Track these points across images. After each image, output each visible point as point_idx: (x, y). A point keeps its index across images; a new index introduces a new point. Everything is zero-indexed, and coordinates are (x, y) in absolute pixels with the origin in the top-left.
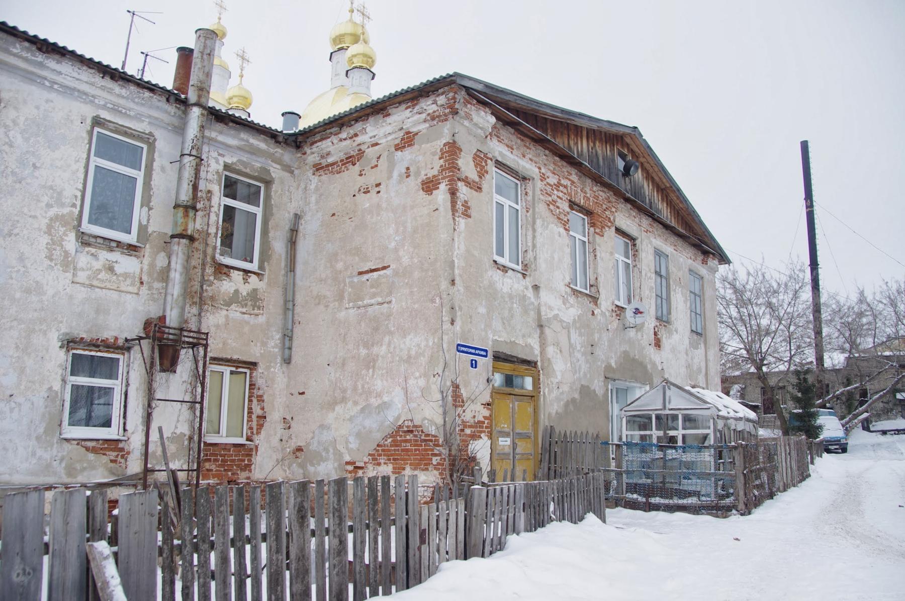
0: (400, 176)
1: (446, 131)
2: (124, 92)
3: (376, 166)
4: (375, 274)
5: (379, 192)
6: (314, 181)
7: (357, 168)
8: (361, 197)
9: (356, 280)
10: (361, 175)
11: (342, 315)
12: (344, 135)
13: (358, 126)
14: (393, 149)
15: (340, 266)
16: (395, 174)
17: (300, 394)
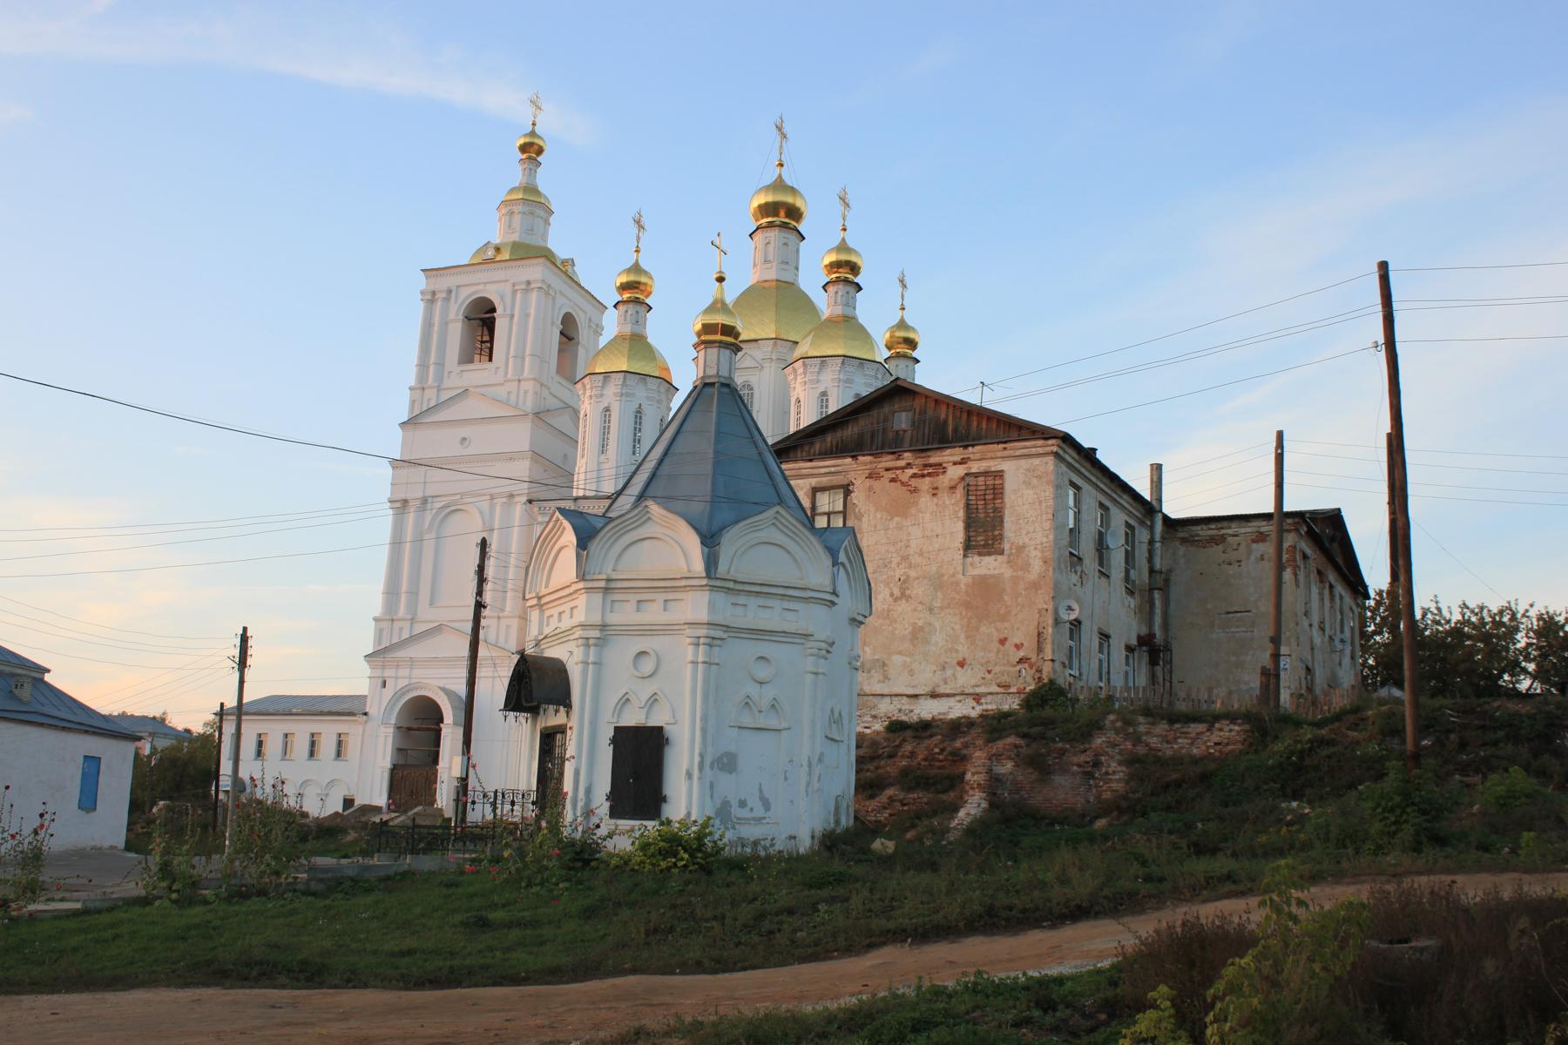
0: (1256, 559)
2: (1134, 505)
3: (1237, 549)
4: (1239, 615)
5: (1240, 566)
6: (1182, 550)
7: (1220, 547)
8: (1225, 567)
9: (1223, 616)
10: (1224, 552)
11: (1214, 636)
12: (1213, 527)
13: (1225, 524)
14: (1249, 542)
15: (1209, 606)
16: (1253, 557)
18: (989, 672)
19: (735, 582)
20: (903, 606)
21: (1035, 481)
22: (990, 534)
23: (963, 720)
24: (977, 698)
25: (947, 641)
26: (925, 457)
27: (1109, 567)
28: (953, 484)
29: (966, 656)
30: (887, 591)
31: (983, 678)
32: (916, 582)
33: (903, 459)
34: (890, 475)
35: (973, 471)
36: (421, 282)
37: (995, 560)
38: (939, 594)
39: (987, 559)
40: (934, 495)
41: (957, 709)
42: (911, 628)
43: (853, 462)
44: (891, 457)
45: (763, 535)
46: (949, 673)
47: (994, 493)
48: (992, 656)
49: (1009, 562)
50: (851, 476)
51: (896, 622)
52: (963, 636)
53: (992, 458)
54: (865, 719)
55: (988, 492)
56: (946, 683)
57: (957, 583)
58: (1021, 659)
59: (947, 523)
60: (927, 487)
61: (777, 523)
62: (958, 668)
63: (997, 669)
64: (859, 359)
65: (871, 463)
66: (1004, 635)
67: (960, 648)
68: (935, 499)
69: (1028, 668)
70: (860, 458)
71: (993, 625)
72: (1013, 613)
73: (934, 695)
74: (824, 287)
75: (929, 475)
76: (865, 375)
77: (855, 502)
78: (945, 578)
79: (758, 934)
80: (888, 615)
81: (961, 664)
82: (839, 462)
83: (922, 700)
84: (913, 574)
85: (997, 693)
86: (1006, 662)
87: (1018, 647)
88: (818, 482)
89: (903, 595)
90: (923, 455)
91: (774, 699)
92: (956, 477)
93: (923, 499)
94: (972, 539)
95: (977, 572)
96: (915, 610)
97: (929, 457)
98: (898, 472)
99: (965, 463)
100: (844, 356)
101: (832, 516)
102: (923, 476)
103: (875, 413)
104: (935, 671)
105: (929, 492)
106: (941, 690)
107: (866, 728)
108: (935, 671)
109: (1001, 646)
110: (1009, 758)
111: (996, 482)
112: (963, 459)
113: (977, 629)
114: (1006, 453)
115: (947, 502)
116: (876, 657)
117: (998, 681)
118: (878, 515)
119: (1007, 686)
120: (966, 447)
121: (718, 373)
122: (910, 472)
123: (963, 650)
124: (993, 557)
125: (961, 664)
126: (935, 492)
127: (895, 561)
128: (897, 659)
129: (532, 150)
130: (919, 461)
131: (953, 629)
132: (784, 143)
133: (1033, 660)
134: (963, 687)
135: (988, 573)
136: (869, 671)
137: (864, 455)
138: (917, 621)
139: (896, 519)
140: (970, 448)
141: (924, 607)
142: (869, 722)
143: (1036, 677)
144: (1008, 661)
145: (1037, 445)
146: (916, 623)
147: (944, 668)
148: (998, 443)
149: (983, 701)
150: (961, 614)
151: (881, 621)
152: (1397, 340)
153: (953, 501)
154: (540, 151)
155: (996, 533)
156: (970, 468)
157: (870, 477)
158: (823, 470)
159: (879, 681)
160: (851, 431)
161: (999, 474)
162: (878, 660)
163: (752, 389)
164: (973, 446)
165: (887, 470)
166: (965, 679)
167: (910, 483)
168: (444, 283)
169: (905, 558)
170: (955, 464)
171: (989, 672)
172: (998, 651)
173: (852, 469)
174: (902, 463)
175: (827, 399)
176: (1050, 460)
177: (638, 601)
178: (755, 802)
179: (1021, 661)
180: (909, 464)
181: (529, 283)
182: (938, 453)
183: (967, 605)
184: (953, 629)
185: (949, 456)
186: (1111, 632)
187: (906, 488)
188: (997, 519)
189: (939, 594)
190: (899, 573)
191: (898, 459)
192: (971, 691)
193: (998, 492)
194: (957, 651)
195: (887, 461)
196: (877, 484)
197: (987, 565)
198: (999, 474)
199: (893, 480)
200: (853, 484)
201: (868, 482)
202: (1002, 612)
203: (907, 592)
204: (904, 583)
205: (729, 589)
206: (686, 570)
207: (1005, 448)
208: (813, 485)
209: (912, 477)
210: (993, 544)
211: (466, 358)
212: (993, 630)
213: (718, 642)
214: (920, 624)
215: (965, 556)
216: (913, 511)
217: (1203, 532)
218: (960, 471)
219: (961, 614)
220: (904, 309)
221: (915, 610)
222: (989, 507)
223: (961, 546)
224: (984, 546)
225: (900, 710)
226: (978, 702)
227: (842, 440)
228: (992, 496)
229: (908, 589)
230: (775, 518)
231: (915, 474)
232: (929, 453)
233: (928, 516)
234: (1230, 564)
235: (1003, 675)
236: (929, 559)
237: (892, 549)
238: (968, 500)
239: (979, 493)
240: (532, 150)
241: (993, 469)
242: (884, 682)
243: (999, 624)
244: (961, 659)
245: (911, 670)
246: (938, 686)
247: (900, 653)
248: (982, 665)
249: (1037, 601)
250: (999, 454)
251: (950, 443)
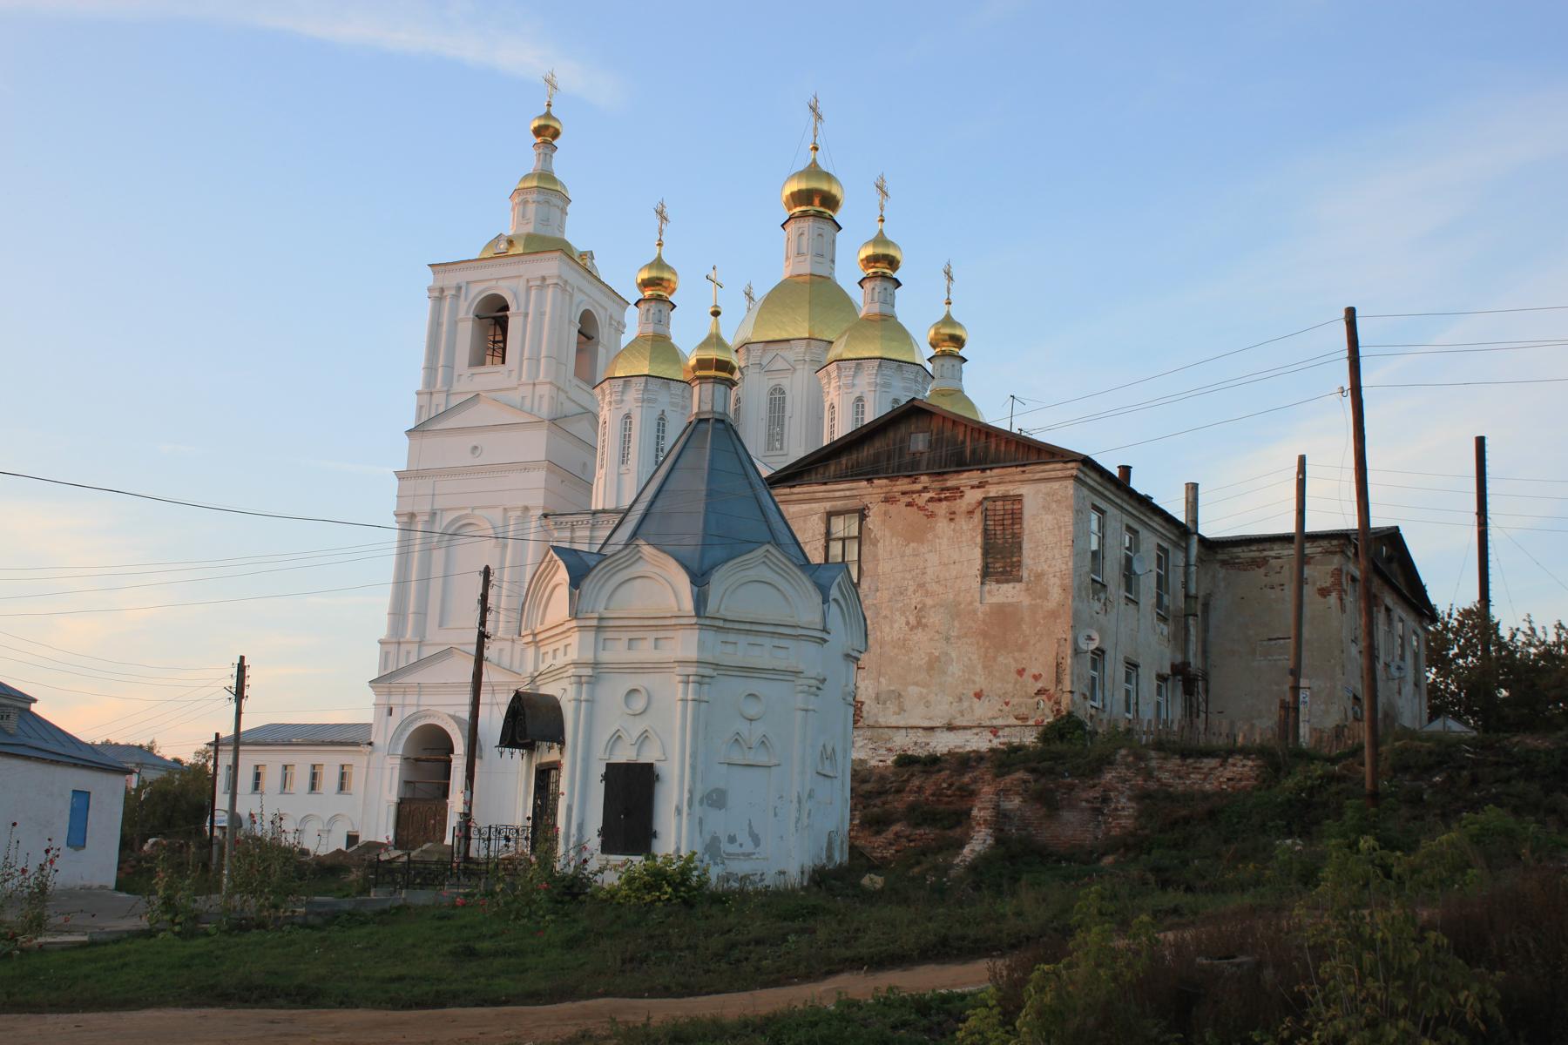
1: (1335, 561)
2: (1167, 527)
4: (1282, 641)
5: (1282, 590)
6: (1222, 573)
7: (1262, 570)
9: (1265, 643)
10: (1266, 576)
12: (1254, 548)
13: (1267, 545)
17: (1219, 712)
18: (1007, 704)
19: (725, 620)
20: (919, 635)
21: (1054, 506)
22: (1008, 560)
23: (972, 755)
24: (994, 731)
25: (964, 672)
27: (1138, 593)
28: (970, 508)
29: (983, 687)
30: (903, 620)
31: (1001, 710)
32: (933, 609)
33: (919, 483)
34: (906, 499)
35: (991, 495)
36: (429, 278)
37: (1014, 588)
38: (956, 623)
39: (1005, 587)
40: (951, 520)
41: (979, 743)
42: (927, 658)
43: (869, 486)
44: (907, 480)
45: (752, 574)
46: (966, 704)
47: (1013, 518)
48: (1010, 687)
49: (1027, 590)
50: (866, 500)
51: (912, 651)
52: (980, 666)
53: (1010, 482)
54: (880, 752)
55: (1006, 517)
56: (963, 716)
57: (975, 612)
58: (1039, 691)
59: (965, 549)
60: (944, 512)
61: (768, 562)
62: (975, 700)
63: (1014, 701)
64: (896, 361)
65: (886, 486)
66: (1023, 666)
67: (977, 679)
68: (953, 525)
69: (1046, 700)
70: (875, 481)
71: (1011, 655)
72: (1032, 642)
73: (951, 728)
74: (860, 283)
75: (946, 499)
76: (903, 379)
77: (871, 527)
78: (962, 606)
79: (726, 962)
80: (904, 645)
81: (978, 695)
82: (854, 485)
83: (938, 733)
84: (929, 602)
85: (1015, 726)
86: (1024, 694)
87: (1036, 678)
88: (832, 506)
89: (919, 623)
90: (940, 478)
91: (764, 736)
92: (973, 502)
93: (939, 524)
94: (990, 565)
95: (994, 600)
96: (931, 639)
97: (946, 480)
98: (914, 496)
99: (983, 487)
100: (881, 358)
101: (847, 542)
102: (940, 500)
103: (891, 434)
104: (951, 703)
105: (945, 517)
106: (958, 722)
107: (881, 761)
108: (951, 703)
109: (1019, 678)
110: (1017, 793)
111: (1015, 507)
112: (980, 483)
113: (995, 659)
115: (965, 528)
116: (892, 688)
117: (1016, 714)
118: (894, 541)
119: (1025, 719)
120: (983, 470)
121: (712, 409)
122: (927, 496)
123: (981, 681)
124: (1011, 585)
125: (978, 695)
126: (953, 516)
127: (911, 589)
128: (913, 690)
129: (547, 133)
130: (937, 485)
131: (970, 659)
132: (819, 125)
133: (1052, 691)
134: (981, 719)
135: (1006, 600)
136: (884, 703)
137: (879, 478)
138: (934, 651)
139: (912, 545)
140: (988, 472)
141: (941, 636)
142: (884, 755)
143: (1054, 709)
144: (1026, 692)
145: (1055, 469)
146: (933, 653)
147: (960, 700)
148: (1017, 466)
149: (1000, 733)
150: (978, 643)
151: (896, 651)
152: (1362, 384)
153: (971, 526)
154: (556, 134)
155: (1015, 559)
156: (989, 492)
157: (886, 500)
158: (842, 494)
159: (895, 713)
160: (867, 452)
161: (1018, 499)
162: (893, 691)
163: (784, 393)
164: (991, 469)
165: (904, 493)
166: (982, 711)
167: (927, 507)
168: (452, 279)
169: (921, 586)
170: (973, 487)
171: (1007, 704)
172: (1016, 683)
173: (867, 492)
174: (918, 487)
175: (863, 405)
176: (1070, 484)
177: (630, 640)
178: (743, 837)
179: (1039, 693)
180: (925, 488)
181: (544, 279)
182: (955, 476)
183: (985, 635)
184: (970, 659)
185: (965, 479)
186: (1140, 661)
187: (923, 512)
188: (1016, 546)
189: (956, 623)
190: (915, 600)
191: (914, 482)
192: (988, 723)
193: (1016, 517)
194: (974, 682)
195: (903, 485)
196: (892, 508)
197: (1005, 593)
198: (1018, 499)
199: (909, 504)
200: (869, 509)
201: (884, 506)
202: (1020, 642)
203: (924, 621)
204: (920, 610)
205: (718, 627)
206: (676, 609)
207: (1024, 472)
208: (828, 509)
209: (929, 501)
210: (1012, 571)
211: (478, 361)
212: (1011, 661)
213: (707, 680)
214: (937, 654)
215: (982, 583)
216: (930, 536)
217: (1244, 554)
218: (978, 495)
219: (978, 643)
220: (950, 303)
221: (931, 639)
222: (1007, 532)
223: (978, 573)
224: (1002, 573)
225: (916, 743)
226: (995, 735)
227: (858, 462)
228: (1010, 521)
229: (924, 617)
230: (766, 556)
231: (931, 498)
232: (946, 477)
233: (945, 541)
234: (1272, 588)
235: (1021, 706)
236: (946, 586)
237: (908, 576)
238: (985, 525)
239: (997, 518)
240: (547, 133)
241: (1011, 493)
242: (899, 714)
243: (1016, 654)
244: (978, 690)
245: (927, 701)
246: (955, 719)
247: (916, 684)
248: (1000, 697)
249: (1056, 631)
251: (969, 465)
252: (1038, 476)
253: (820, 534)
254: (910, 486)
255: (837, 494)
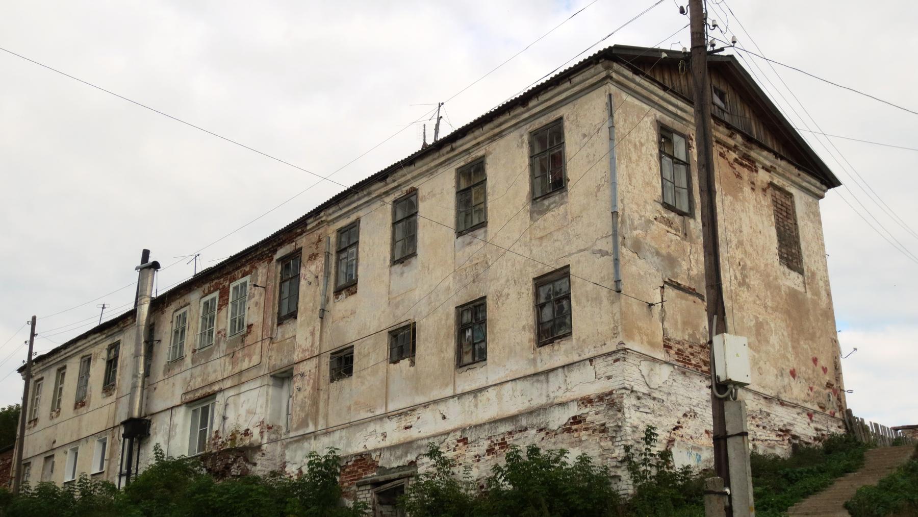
25: (780, 346)
26: (748, 148)
29: (795, 366)
33: (734, 139)
112: (771, 167)
114: (798, 180)
174: (731, 142)
191: (730, 136)
203: (747, 280)
245: (760, 368)
250: (793, 178)
252: (805, 184)
253: (653, 141)
254: (726, 137)
255: (671, 108)
